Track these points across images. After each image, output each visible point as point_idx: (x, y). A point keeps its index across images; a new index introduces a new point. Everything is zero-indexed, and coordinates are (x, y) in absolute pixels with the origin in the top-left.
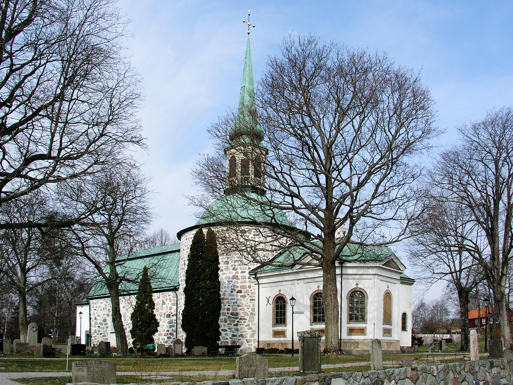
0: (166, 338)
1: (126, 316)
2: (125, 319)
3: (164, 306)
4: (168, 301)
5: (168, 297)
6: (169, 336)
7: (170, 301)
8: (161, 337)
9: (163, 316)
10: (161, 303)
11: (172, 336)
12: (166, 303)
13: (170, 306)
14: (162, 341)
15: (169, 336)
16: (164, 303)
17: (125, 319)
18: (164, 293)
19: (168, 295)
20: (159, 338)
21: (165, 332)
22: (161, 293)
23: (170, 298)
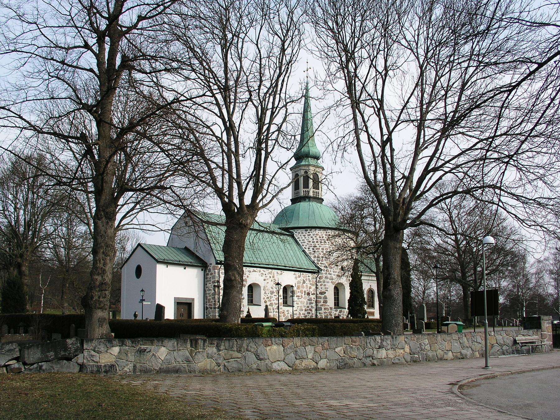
0: (306, 313)
1: (266, 288)
2: (265, 292)
3: (305, 285)
4: (308, 281)
5: (308, 278)
6: (309, 311)
7: (310, 281)
8: (302, 312)
9: (304, 293)
10: (302, 282)
11: (311, 312)
12: (306, 282)
13: (309, 285)
14: (303, 316)
15: (309, 311)
16: (304, 282)
17: (265, 292)
18: (304, 273)
19: (307, 275)
20: (300, 313)
21: (306, 308)
22: (301, 273)
23: (309, 279)
